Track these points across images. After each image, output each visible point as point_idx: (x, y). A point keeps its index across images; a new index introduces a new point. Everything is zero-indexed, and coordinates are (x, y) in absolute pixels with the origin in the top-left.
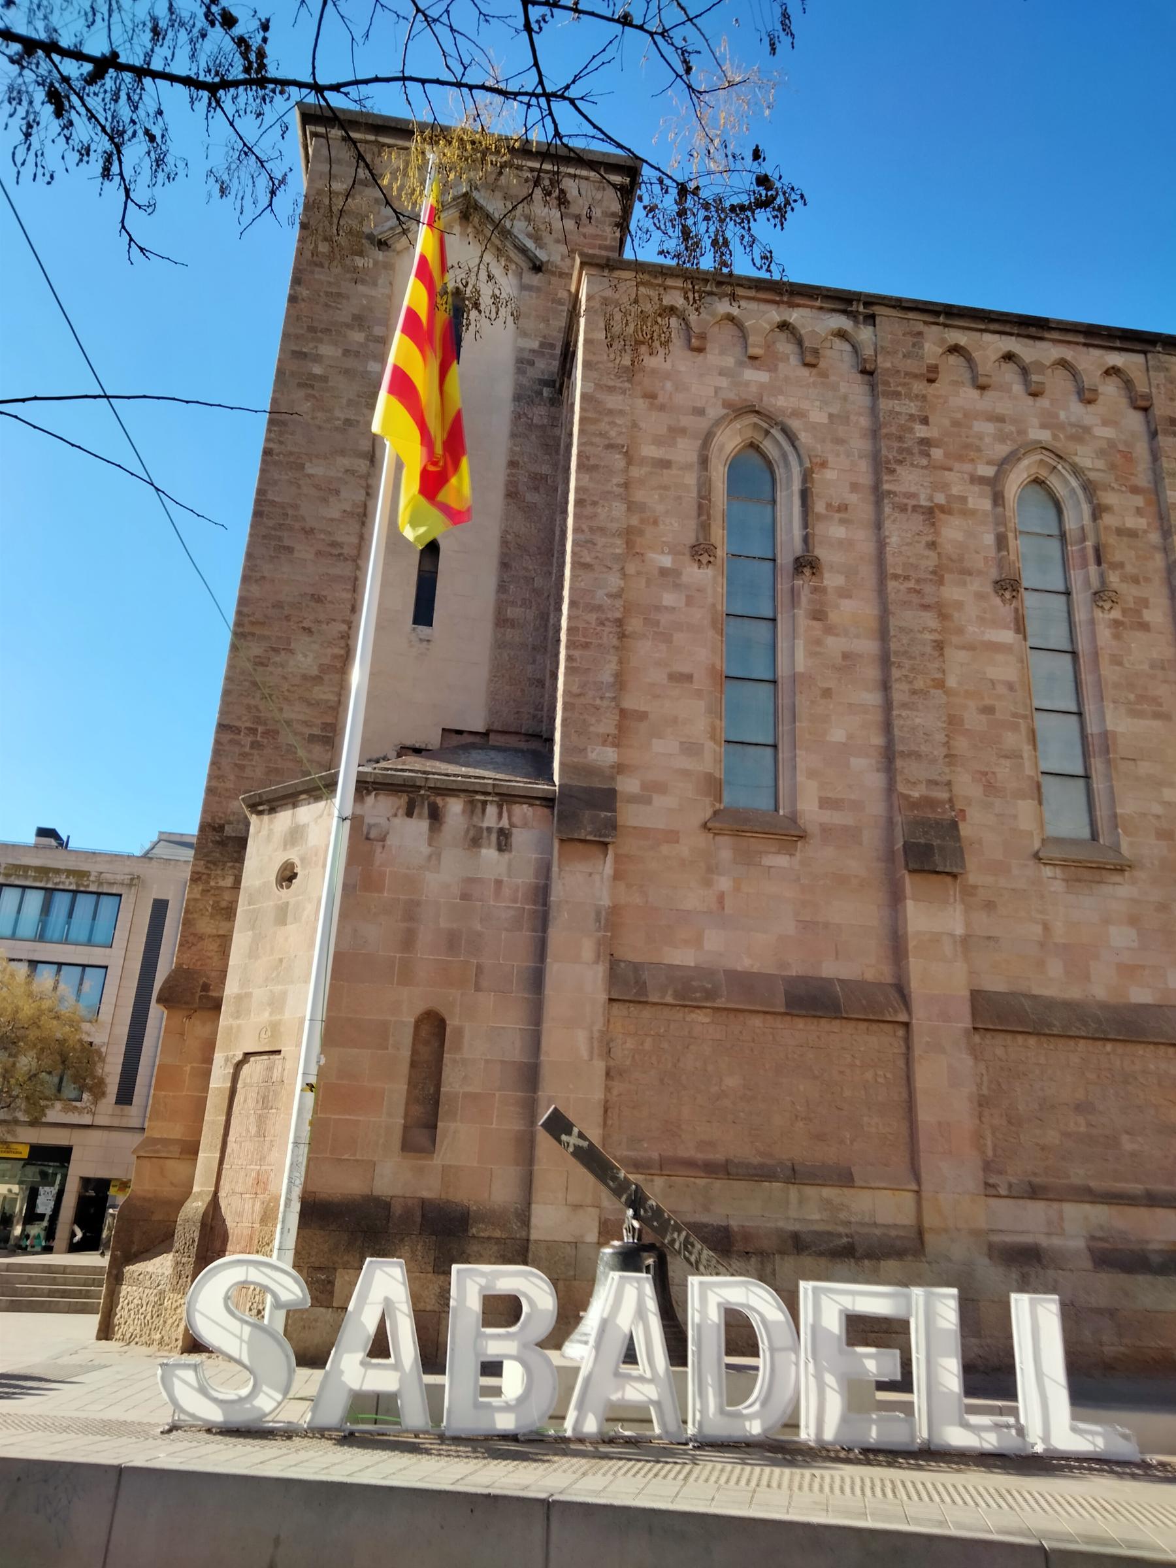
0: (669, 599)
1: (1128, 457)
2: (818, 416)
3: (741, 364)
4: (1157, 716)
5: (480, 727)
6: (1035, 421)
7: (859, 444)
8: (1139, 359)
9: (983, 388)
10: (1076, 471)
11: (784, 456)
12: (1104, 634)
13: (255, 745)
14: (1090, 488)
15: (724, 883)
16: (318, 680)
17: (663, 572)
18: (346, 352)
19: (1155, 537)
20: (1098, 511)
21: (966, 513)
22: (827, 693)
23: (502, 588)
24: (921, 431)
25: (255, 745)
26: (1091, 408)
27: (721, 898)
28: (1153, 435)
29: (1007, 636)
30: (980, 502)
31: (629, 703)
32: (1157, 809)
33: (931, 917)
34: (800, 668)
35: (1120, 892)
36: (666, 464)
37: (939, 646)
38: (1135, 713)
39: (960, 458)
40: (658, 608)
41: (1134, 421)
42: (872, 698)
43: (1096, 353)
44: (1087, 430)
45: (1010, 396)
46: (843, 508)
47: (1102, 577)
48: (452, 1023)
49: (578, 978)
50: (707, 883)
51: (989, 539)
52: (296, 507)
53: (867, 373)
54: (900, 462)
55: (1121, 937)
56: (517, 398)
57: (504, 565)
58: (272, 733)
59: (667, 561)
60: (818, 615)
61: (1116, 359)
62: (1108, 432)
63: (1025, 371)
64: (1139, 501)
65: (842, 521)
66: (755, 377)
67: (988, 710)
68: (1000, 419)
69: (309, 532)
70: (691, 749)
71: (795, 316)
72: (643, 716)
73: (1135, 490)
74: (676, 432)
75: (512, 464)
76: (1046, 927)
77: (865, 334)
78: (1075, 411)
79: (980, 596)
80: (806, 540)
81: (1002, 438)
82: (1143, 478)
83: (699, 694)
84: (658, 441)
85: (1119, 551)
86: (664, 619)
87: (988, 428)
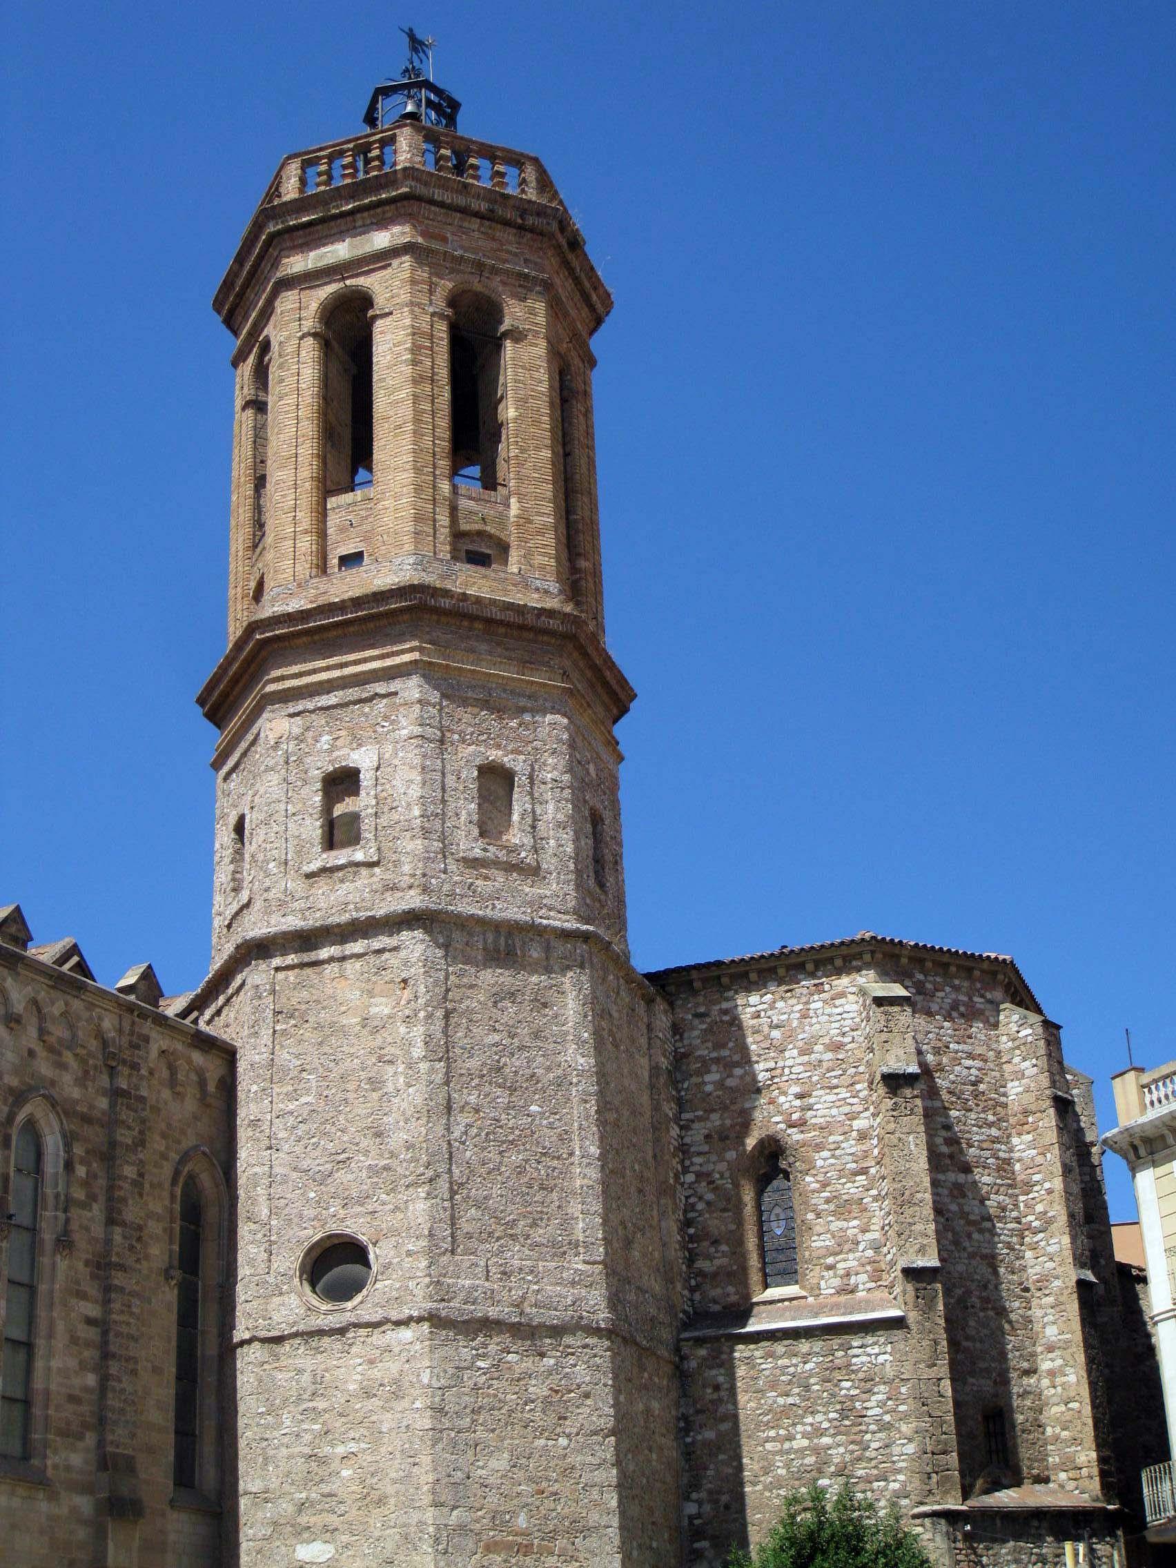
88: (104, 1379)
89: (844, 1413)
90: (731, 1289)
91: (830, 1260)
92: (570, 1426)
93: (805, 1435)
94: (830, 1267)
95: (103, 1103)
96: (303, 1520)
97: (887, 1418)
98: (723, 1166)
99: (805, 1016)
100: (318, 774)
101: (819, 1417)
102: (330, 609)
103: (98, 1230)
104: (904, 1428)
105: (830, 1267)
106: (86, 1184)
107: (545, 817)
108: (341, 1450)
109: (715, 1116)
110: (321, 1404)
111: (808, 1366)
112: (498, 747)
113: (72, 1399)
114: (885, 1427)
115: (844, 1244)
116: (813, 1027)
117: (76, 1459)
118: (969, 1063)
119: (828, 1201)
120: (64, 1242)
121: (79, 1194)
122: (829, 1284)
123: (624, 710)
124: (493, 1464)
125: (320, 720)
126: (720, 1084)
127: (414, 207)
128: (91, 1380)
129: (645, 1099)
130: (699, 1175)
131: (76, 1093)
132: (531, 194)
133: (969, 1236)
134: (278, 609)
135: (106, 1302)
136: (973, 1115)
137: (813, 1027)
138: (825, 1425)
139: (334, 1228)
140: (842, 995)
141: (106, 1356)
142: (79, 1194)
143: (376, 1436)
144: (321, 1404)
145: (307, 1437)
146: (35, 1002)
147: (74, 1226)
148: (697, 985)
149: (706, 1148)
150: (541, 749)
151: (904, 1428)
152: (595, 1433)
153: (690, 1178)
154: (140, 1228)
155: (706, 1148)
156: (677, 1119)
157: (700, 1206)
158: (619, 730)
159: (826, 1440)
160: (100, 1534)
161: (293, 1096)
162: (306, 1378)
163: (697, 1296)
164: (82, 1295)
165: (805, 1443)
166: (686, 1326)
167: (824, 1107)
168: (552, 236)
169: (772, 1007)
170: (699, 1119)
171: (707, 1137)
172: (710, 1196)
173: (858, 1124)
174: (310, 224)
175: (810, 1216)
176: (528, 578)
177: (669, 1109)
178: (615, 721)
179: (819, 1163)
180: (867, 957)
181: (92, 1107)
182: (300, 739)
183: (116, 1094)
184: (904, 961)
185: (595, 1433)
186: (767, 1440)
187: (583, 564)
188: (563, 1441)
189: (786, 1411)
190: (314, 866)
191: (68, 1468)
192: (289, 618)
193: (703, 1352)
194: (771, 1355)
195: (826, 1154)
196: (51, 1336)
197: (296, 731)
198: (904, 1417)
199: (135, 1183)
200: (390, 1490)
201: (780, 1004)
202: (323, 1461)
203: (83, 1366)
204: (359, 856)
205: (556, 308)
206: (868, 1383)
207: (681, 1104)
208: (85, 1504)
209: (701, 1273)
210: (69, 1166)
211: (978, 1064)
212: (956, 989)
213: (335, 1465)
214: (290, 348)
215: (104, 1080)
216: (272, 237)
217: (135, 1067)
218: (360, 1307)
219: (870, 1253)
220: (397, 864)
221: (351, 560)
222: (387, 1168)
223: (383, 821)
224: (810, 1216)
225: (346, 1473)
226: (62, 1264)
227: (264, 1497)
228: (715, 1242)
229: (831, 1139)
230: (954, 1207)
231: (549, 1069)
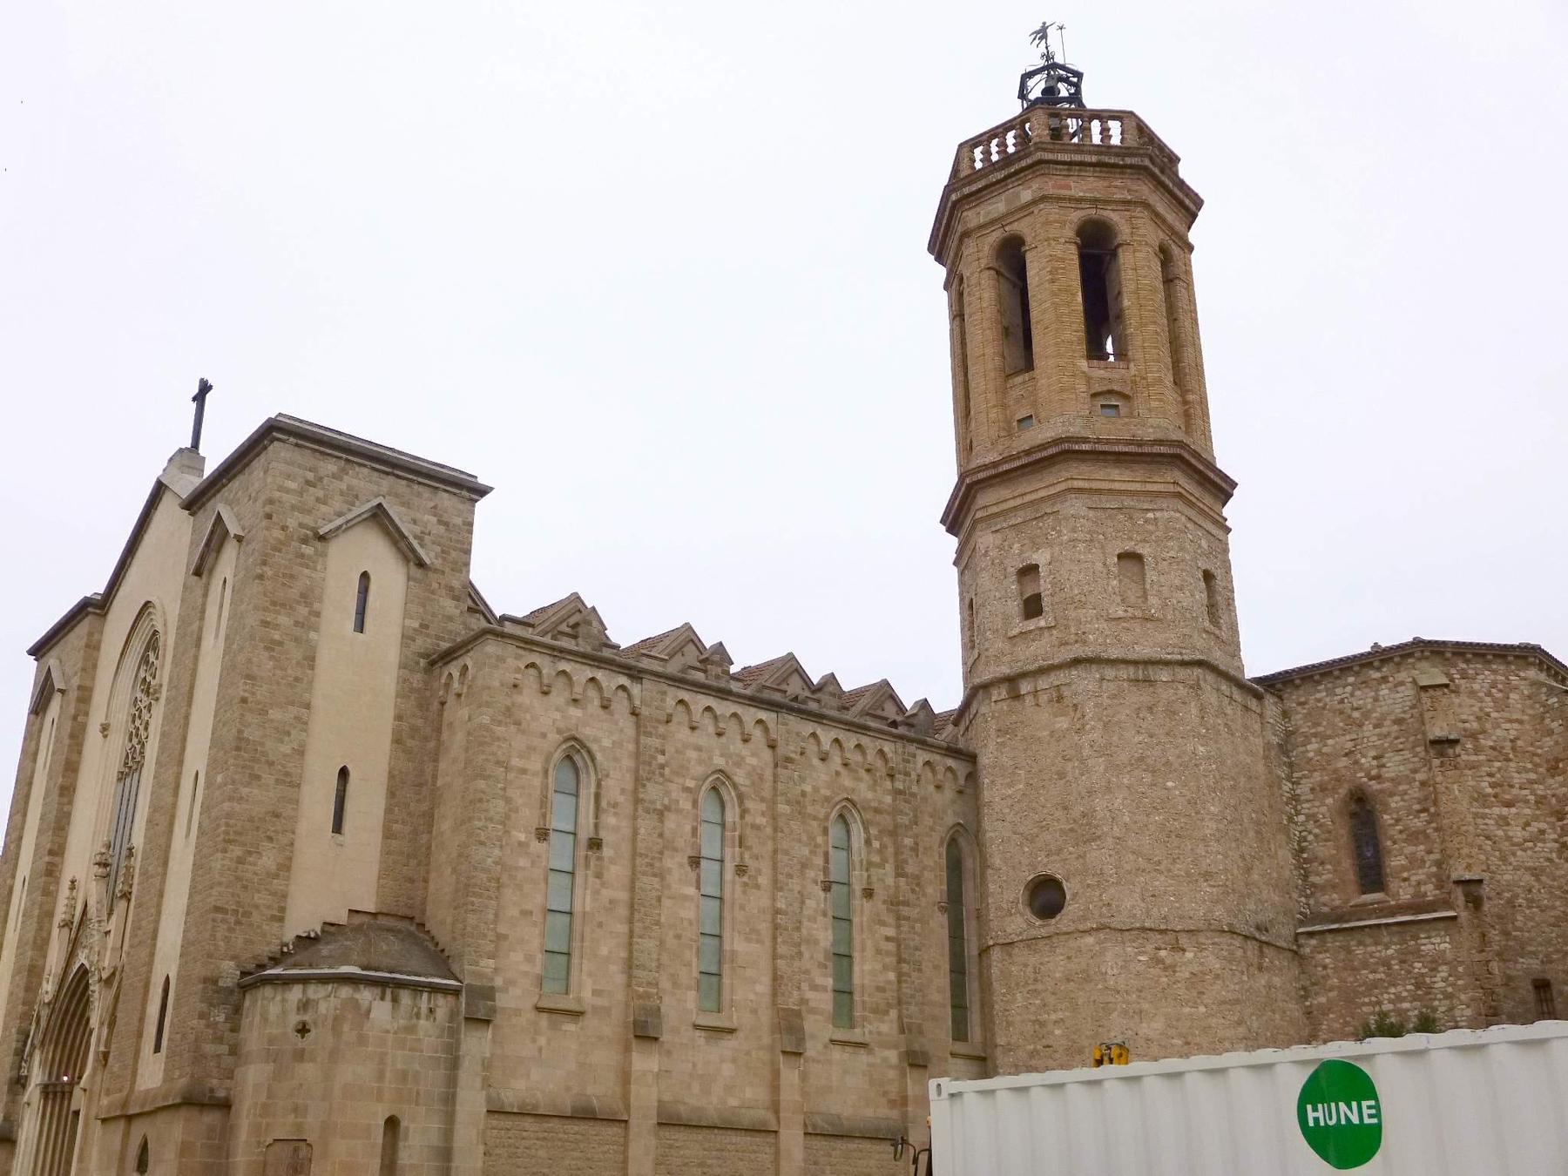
0: (523, 862)
1: (761, 777)
2: (607, 743)
3: (567, 703)
4: (758, 941)
5: (371, 908)
6: (717, 752)
7: (628, 763)
8: (774, 715)
9: (693, 728)
10: (735, 786)
11: (587, 767)
12: (738, 889)
13: (238, 923)
14: (741, 798)
15: (542, 1041)
16: (277, 876)
17: (520, 844)
18: (297, 623)
19: (769, 830)
20: (744, 812)
21: (679, 811)
22: (600, 925)
23: (389, 810)
24: (661, 759)
25: (238, 923)
26: (749, 745)
27: (540, 1049)
28: (776, 766)
29: (691, 891)
30: (686, 805)
31: (502, 929)
32: (752, 997)
33: (644, 1062)
34: (588, 909)
35: (728, 1044)
36: (524, 771)
37: (659, 899)
38: (748, 940)
39: (677, 774)
40: (516, 868)
41: (767, 755)
42: (622, 928)
43: (752, 710)
44: (743, 758)
45: (705, 737)
46: (615, 805)
47: (742, 854)
48: (404, 1124)
49: (471, 1101)
50: (534, 1041)
51: (688, 828)
52: (262, 744)
53: (634, 713)
54: (649, 780)
55: (727, 1069)
56: (403, 666)
57: (391, 794)
58: (247, 914)
59: (522, 837)
60: (599, 875)
61: (763, 715)
62: (752, 761)
63: (716, 718)
64: (763, 806)
65: (616, 814)
66: (575, 712)
67: (678, 937)
68: (698, 749)
69: (271, 764)
70: (529, 959)
71: (600, 675)
72: (505, 937)
73: (763, 800)
74: (532, 749)
75: (399, 717)
76: (694, 1065)
77: (636, 689)
78: (737, 746)
79: (681, 865)
80: (596, 826)
81: (700, 762)
82: (767, 792)
83: (535, 924)
84: (521, 757)
85: (751, 840)
86: (520, 875)
87: (692, 754)
88: (900, 976)
89: (1418, 986)
90: (1335, 896)
91: (1405, 875)
92: (1207, 999)
93: (1390, 1001)
94: (1405, 880)
95: (888, 799)
96: (1033, 1062)
97: (1450, 990)
98: (1324, 809)
99: (1376, 700)
100: (1011, 570)
101: (1400, 988)
102: (1011, 458)
103: (890, 881)
104: (1463, 997)
105: (1405, 880)
106: (880, 851)
108: (1054, 1017)
109: (1316, 774)
110: (1040, 987)
111: (1390, 952)
112: (1131, 539)
113: (880, 989)
114: (1448, 996)
115: (1415, 862)
117: (884, 1028)
118: (1508, 726)
119: (1401, 832)
120: (869, 893)
121: (876, 859)
123: (1229, 496)
124: (1154, 1025)
125: (1011, 534)
126: (1319, 752)
127: (1044, 169)
128: (892, 976)
129: (1260, 768)
130: (1308, 817)
131: (870, 795)
132: (1132, 141)
133: (1514, 854)
134: (980, 461)
135: (898, 927)
136: (1512, 764)
138: (1405, 994)
139: (1043, 870)
140: (1402, 683)
141: (900, 960)
142: (876, 859)
144: (1040, 987)
145: (1033, 1009)
146: (837, 740)
147: (874, 879)
148: (1298, 682)
149: (1311, 797)
151: (1463, 997)
152: (1224, 1002)
153: (1302, 818)
154: (918, 877)
155: (1311, 797)
156: (1289, 778)
157: (1310, 838)
158: (1227, 511)
159: (1406, 1005)
160: (903, 1075)
161: (1011, 785)
162: (1030, 969)
163: (1312, 902)
164: (883, 924)
165: (1391, 1007)
166: (1301, 923)
168: (1146, 168)
169: (1352, 695)
170: (1305, 777)
171: (1312, 789)
172: (1317, 831)
173: (1420, 776)
174: (979, 191)
175: (1389, 843)
177: (1282, 772)
178: (1224, 504)
179: (1393, 805)
180: (1418, 655)
181: (880, 802)
182: (1000, 548)
183: (897, 793)
184: (1448, 655)
185: (1224, 1002)
186: (1364, 1004)
187: (1191, 397)
188: (1202, 1009)
189: (1375, 984)
190: (1015, 632)
191: (879, 1033)
192: (985, 467)
193: (1313, 942)
194: (1360, 943)
195: (1397, 798)
196: (863, 950)
197: (998, 542)
198: (1464, 989)
199: (912, 849)
200: (1085, 1043)
201: (1358, 693)
202: (1042, 1024)
203: (885, 968)
204: (1042, 623)
206: (1434, 964)
207: (1291, 765)
208: (893, 1056)
209: (1313, 885)
210: (868, 842)
211: (1516, 726)
212: (1494, 672)
213: (1050, 1027)
214: (973, 281)
215: (888, 784)
216: (955, 204)
217: (907, 774)
218: (1062, 921)
219: (1434, 869)
220: (1067, 627)
222: (1072, 830)
223: (1056, 599)
224: (1389, 843)
225: (1057, 1032)
226: (867, 905)
227: (1009, 1048)
228: (1322, 863)
229: (1401, 788)
230: (1500, 833)
231: (1179, 757)
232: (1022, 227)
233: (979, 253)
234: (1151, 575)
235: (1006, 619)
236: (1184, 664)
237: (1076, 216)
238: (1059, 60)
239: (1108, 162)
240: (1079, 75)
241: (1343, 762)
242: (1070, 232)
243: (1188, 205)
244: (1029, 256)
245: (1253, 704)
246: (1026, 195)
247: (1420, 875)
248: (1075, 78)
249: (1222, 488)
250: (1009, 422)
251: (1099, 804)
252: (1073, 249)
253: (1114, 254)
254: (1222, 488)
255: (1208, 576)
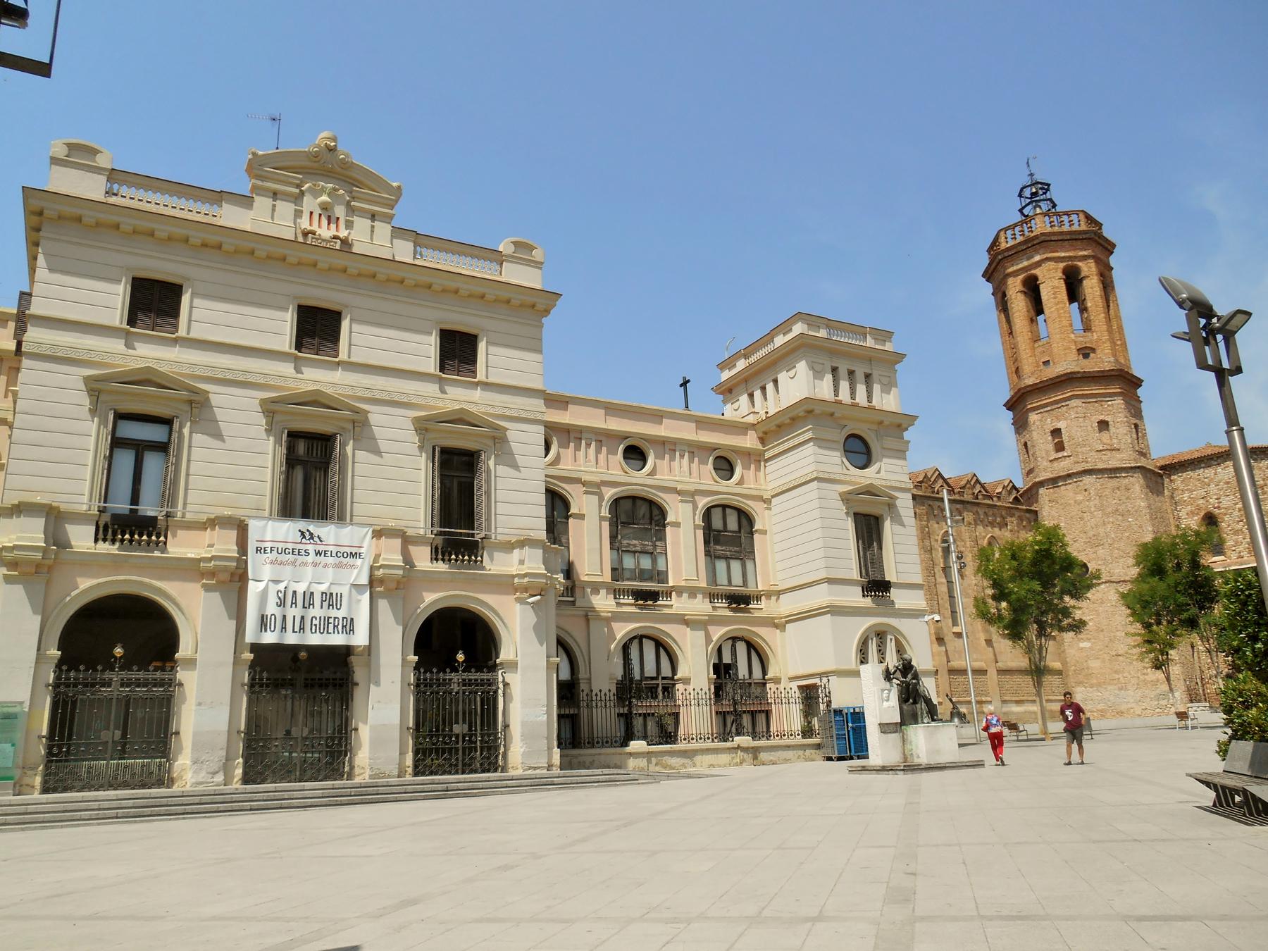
61: (958, 506)
107: (1121, 430)
115: (1237, 543)
116: (1220, 477)
122: (1234, 556)
132: (1084, 227)
137: (1220, 477)
143: (1098, 615)
150: (1115, 409)
158: (1140, 392)
167: (1225, 502)
176: (1103, 361)
205: (1098, 261)
221: (1046, 363)
232: (1036, 272)
233: (1014, 286)
234: (1112, 429)
235: (1047, 452)
236: (1132, 468)
237: (1062, 265)
238: (1038, 178)
239: (1074, 238)
240: (1049, 185)
241: (1202, 501)
242: (1060, 274)
243: (1108, 247)
244: (1041, 287)
245: (1159, 480)
246: (1037, 258)
247: (1241, 548)
248: (1046, 187)
249: (1136, 383)
250: (1037, 363)
251: (1101, 531)
252: (1062, 282)
253: (1081, 281)
254: (1136, 383)
255: (1136, 426)
